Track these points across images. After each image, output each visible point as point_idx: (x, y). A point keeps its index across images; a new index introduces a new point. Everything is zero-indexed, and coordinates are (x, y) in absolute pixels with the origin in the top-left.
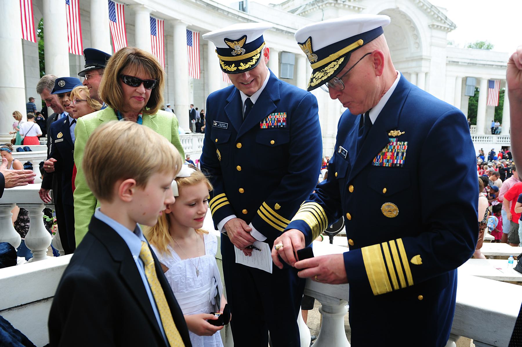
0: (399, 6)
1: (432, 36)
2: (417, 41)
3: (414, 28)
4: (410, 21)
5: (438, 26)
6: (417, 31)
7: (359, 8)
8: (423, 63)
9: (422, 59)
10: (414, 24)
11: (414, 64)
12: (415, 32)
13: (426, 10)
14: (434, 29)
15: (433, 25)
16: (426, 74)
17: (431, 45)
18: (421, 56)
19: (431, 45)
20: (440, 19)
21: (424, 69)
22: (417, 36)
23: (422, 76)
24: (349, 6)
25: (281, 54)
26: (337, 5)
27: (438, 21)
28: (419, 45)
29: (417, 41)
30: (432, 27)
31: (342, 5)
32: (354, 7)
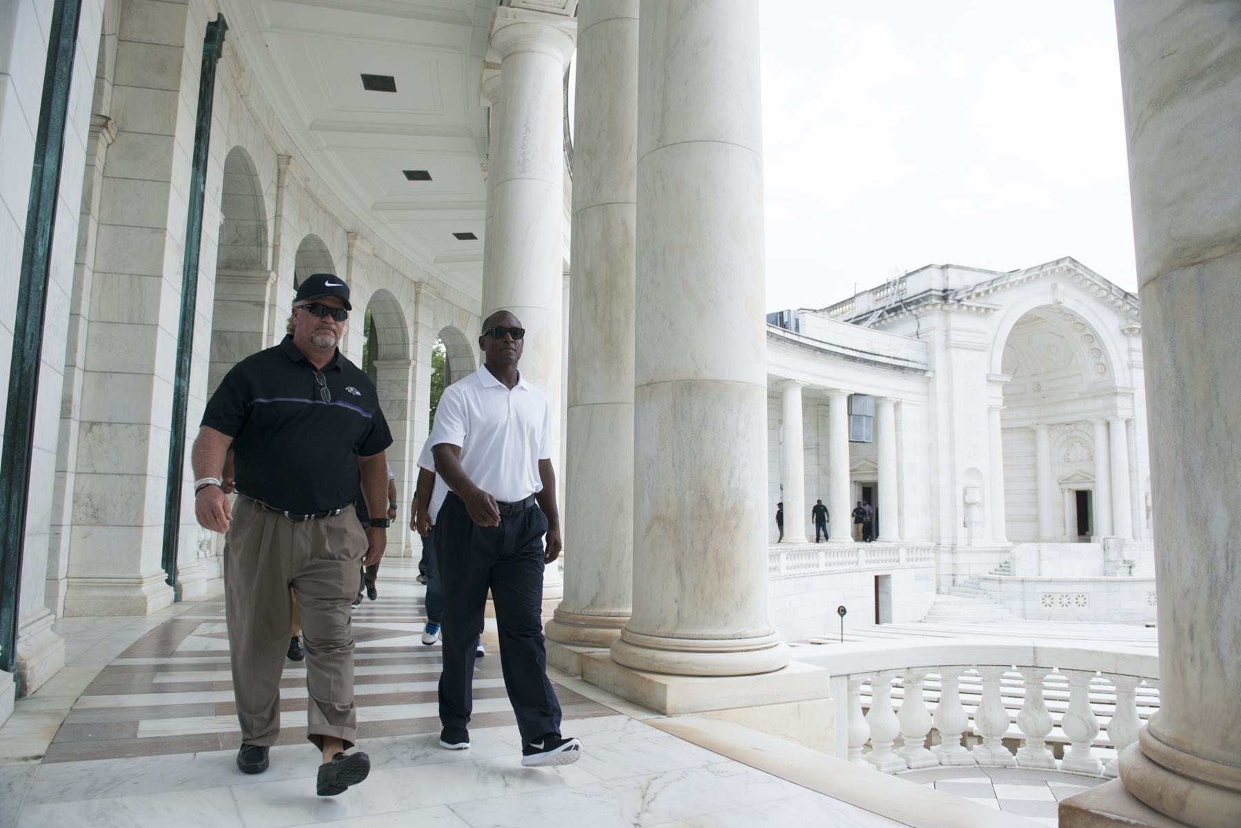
0: (1060, 299)
1: (1130, 350)
2: (1102, 360)
3: (1092, 337)
4: (1083, 325)
6: (1101, 342)
7: (987, 309)
8: (1121, 402)
9: (1116, 394)
10: (1092, 329)
11: (1099, 403)
12: (1096, 345)
13: (1113, 302)
15: (1131, 330)
16: (1127, 422)
17: (1131, 366)
18: (1114, 388)
19: (1131, 366)
21: (1123, 413)
22: (1100, 352)
23: (1119, 429)
24: (969, 307)
25: (850, 398)
26: (946, 308)
28: (1106, 368)
29: (1102, 360)
31: (956, 306)
32: (978, 309)
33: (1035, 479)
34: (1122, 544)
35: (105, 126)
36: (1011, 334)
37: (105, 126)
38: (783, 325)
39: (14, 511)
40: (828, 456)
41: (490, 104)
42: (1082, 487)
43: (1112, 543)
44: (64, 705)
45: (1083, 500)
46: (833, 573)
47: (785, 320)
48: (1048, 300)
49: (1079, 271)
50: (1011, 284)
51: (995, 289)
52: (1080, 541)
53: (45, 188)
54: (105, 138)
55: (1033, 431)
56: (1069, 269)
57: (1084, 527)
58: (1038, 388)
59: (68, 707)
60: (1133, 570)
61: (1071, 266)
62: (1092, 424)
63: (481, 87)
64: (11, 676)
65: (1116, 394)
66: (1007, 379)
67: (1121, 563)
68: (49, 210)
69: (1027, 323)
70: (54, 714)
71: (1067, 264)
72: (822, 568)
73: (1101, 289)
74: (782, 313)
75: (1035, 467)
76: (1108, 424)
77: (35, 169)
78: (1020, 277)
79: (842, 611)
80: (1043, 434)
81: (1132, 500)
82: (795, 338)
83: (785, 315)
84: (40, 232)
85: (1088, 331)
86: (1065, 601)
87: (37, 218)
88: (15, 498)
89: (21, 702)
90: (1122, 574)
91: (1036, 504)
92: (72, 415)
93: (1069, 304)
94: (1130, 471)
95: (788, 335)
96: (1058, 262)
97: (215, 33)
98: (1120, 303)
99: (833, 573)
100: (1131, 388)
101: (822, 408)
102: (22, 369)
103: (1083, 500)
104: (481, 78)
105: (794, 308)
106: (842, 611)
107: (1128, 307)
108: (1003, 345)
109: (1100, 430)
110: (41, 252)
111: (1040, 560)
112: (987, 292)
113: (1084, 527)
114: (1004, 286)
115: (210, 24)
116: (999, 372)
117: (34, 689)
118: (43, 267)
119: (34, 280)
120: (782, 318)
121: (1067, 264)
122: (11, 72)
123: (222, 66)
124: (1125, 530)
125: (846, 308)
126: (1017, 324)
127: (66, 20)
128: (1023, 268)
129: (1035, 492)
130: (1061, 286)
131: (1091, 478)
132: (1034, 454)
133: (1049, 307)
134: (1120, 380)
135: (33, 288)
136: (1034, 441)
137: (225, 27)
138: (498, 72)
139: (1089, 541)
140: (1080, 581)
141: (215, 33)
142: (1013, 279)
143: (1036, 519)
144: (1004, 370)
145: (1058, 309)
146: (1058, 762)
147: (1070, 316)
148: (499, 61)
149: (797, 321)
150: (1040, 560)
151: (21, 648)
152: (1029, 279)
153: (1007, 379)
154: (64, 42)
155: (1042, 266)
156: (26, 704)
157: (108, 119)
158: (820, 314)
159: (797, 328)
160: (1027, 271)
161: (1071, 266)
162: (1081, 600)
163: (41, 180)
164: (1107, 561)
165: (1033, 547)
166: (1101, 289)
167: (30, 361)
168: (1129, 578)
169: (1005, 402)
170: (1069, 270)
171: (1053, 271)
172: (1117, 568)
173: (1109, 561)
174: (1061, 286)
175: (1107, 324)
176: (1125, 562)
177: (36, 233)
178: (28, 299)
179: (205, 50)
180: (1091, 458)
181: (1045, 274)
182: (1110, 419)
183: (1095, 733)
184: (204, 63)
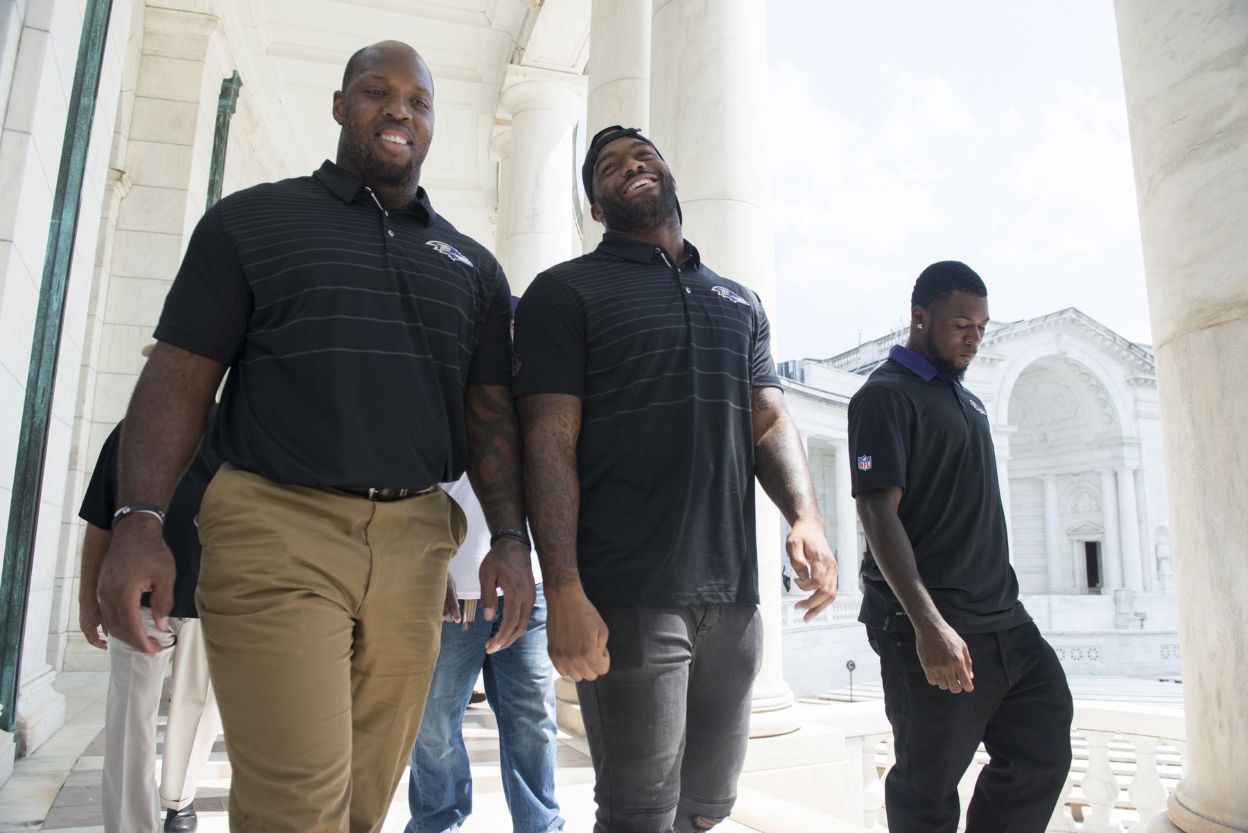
1: (1136, 400)
2: (1108, 410)
3: (1098, 387)
4: (1088, 375)
5: (1146, 380)
7: (992, 360)
8: (1127, 451)
9: (1123, 444)
10: (1098, 380)
13: (1117, 353)
14: (1140, 386)
15: (1137, 380)
16: (1135, 473)
17: (1137, 416)
19: (1137, 416)
20: (1148, 367)
21: (1131, 463)
22: (1106, 402)
23: (1127, 480)
27: (1145, 371)
28: (1112, 419)
29: (1108, 410)
30: (1134, 382)
33: (1044, 530)
34: (1133, 597)
35: (120, 179)
36: (1017, 385)
37: (120, 179)
38: (788, 376)
39: (20, 568)
40: (835, 507)
41: (499, 159)
42: (1091, 538)
43: (1122, 594)
44: (65, 767)
45: (1092, 551)
46: (841, 626)
47: (791, 370)
48: (1053, 350)
49: (1083, 321)
50: (1016, 335)
51: (999, 340)
52: (1090, 593)
53: (61, 243)
54: (120, 190)
55: (1041, 482)
56: (1072, 319)
57: (1094, 578)
58: (1044, 438)
59: (68, 768)
60: (1145, 623)
61: (1074, 316)
62: (1099, 474)
63: (491, 143)
64: (11, 736)
65: (1123, 444)
66: (1014, 429)
67: (1132, 616)
68: (65, 265)
69: (1032, 373)
70: (54, 776)
71: (1071, 314)
72: (830, 622)
73: (1105, 339)
74: (787, 364)
75: (1043, 518)
76: (1116, 474)
77: (52, 224)
78: (1024, 327)
79: (851, 666)
80: (1050, 485)
81: (1141, 551)
82: (801, 389)
83: (790, 366)
84: (55, 286)
85: (1093, 382)
86: (1076, 654)
87: (52, 273)
88: (21, 553)
89: (21, 762)
90: (1133, 628)
91: (1045, 555)
92: (78, 467)
93: (1074, 354)
94: (1139, 522)
95: (793, 386)
96: (1061, 313)
97: (230, 89)
98: (1125, 353)
99: (841, 626)
100: (1139, 438)
101: (829, 459)
102: (33, 423)
103: (1092, 551)
104: (491, 132)
105: (799, 358)
106: (851, 666)
107: (1132, 357)
108: (1008, 396)
109: (1108, 480)
110: (55, 306)
111: (1050, 613)
112: (992, 342)
113: (1094, 578)
114: (1008, 336)
115: (225, 80)
116: (1005, 422)
117: (33, 749)
118: (57, 322)
119: (48, 335)
120: (787, 369)
121: (1071, 314)
122: (33, 132)
123: (235, 121)
124: (1135, 582)
125: (850, 358)
126: (1022, 374)
127: (87, 79)
128: (1027, 318)
129: (1044, 543)
130: (1065, 337)
131: (1100, 529)
132: (1042, 505)
133: (1053, 358)
134: (1127, 429)
135: (46, 342)
136: (1042, 492)
137: (240, 84)
138: (509, 128)
139: (1099, 593)
140: (1092, 635)
141: (230, 89)
142: (1017, 329)
143: (1046, 570)
144: (1011, 421)
145: (1062, 358)
146: (1078, 826)
147: (1076, 365)
148: (509, 117)
149: (802, 371)
150: (1050, 613)
151: (21, 706)
152: (1033, 329)
153: (1014, 429)
154: (85, 101)
155: (1046, 317)
156: (25, 765)
157: (123, 173)
158: (825, 365)
159: (802, 379)
160: (1031, 322)
161: (1074, 316)
162: (1093, 654)
163: (58, 235)
164: (1119, 613)
165: (1043, 599)
166: (1105, 339)
167: (40, 415)
168: (1139, 630)
169: (1011, 453)
170: (1073, 321)
171: (1056, 322)
172: (1129, 621)
173: (1120, 613)
174: (1065, 337)
175: (1113, 375)
176: (1136, 614)
177: (51, 288)
178: (41, 353)
179: (220, 106)
180: (1100, 509)
181: (1049, 324)
182: (1118, 469)
183: (1116, 795)
184: (218, 119)
